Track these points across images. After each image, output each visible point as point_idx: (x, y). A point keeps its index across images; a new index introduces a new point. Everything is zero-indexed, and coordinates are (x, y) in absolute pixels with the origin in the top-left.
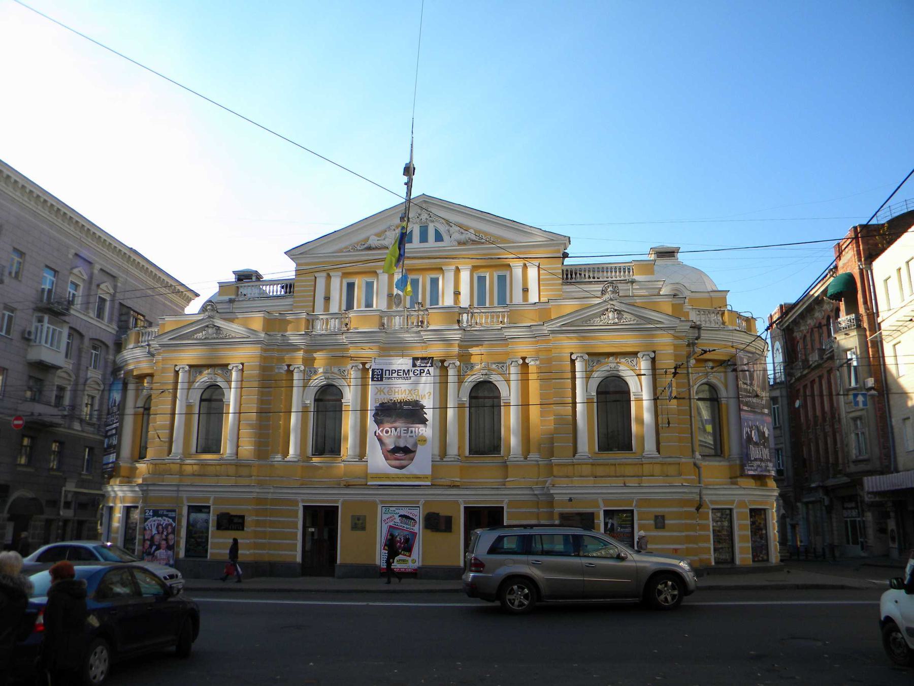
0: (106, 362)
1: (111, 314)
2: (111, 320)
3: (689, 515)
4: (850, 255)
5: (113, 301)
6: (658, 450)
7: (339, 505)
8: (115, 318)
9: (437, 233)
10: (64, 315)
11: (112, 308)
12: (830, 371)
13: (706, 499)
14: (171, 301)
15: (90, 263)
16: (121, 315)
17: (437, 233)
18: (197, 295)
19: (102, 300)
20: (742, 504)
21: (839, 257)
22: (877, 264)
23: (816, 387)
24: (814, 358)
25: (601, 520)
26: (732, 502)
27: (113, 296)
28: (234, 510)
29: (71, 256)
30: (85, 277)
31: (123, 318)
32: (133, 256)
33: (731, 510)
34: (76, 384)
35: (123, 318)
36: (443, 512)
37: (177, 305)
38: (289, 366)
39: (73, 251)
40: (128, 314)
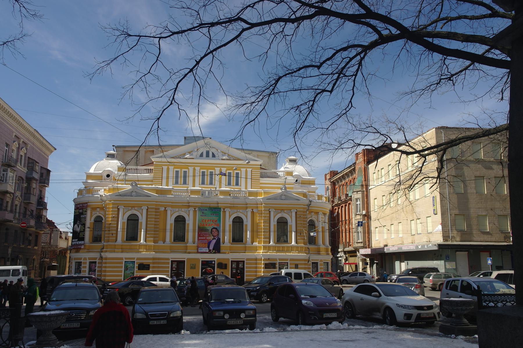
0: (22, 188)
1: (25, 163)
2: (24, 166)
3: (305, 264)
4: (361, 159)
5: (25, 157)
6: (297, 243)
7: (186, 260)
8: (26, 165)
9: (213, 154)
10: (14, 167)
11: (25, 159)
12: (349, 204)
13: (311, 259)
14: (44, 153)
15: (19, 138)
16: (29, 163)
17: (213, 154)
18: (55, 149)
19: (21, 156)
20: (321, 261)
21: (357, 159)
22: (370, 166)
23: (343, 209)
24: (343, 198)
25: (277, 266)
26: (318, 260)
27: (25, 154)
28: (145, 262)
29: (13, 137)
30: (18, 146)
31: (30, 165)
32: (36, 134)
33: (317, 263)
34: (13, 199)
35: (30, 165)
36: (224, 262)
37: (46, 155)
38: (165, 208)
39: (14, 134)
40: (33, 163)
